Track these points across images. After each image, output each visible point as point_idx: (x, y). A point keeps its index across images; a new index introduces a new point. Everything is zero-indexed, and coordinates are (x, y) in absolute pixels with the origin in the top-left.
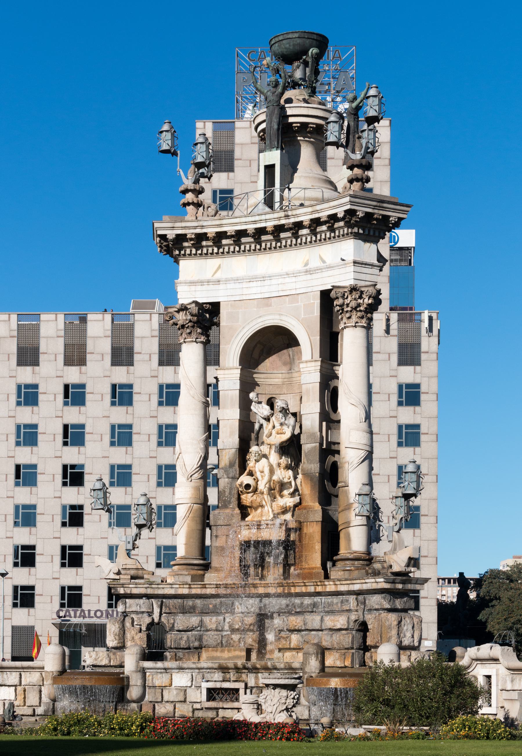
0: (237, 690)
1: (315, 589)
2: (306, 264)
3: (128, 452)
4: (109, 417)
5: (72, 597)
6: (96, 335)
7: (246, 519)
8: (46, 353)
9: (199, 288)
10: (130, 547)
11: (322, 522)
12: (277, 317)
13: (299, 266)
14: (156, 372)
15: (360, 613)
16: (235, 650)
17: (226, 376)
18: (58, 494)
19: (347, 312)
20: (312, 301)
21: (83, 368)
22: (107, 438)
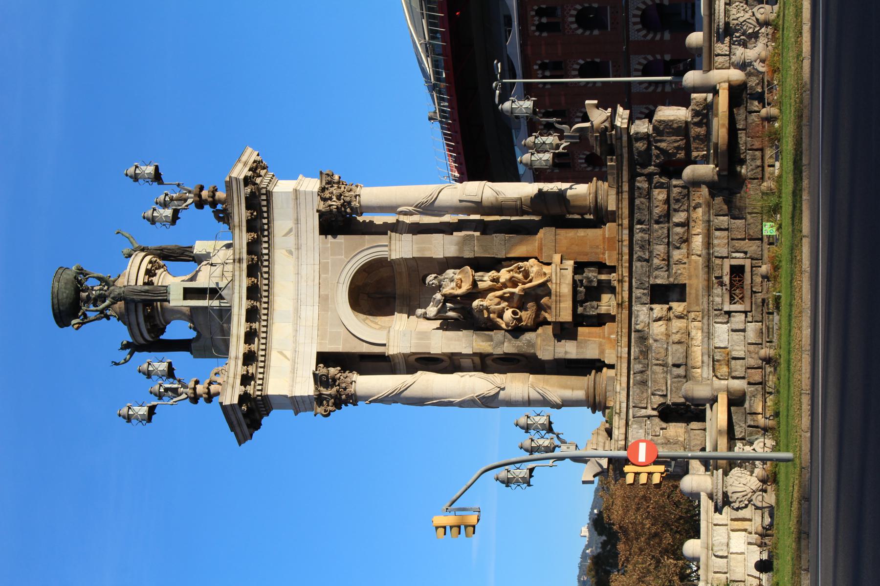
0: (732, 267)
2: (291, 253)
9: (300, 372)
11: (557, 227)
12: (341, 285)
13: (291, 260)
17: (396, 344)
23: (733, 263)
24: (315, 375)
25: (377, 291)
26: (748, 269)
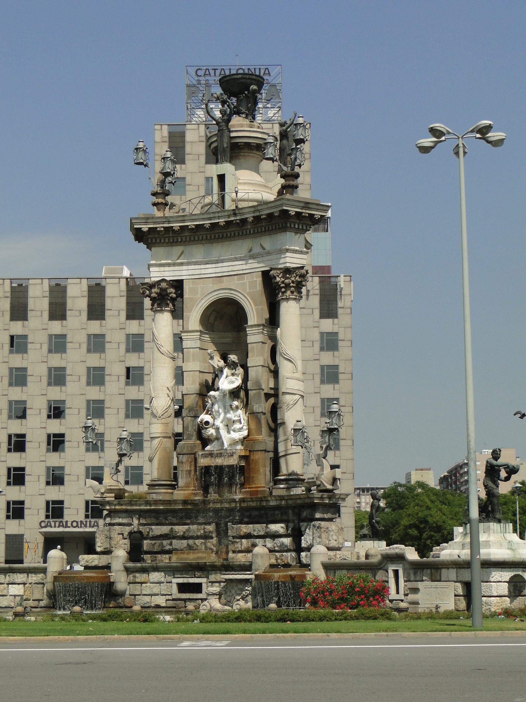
0: (200, 584)
1: (261, 503)
2: (250, 251)
3: (101, 391)
4: (85, 362)
5: (55, 510)
6: (75, 295)
7: (206, 449)
8: (34, 310)
9: (167, 269)
10: (114, 471)
12: (229, 291)
14: (124, 325)
15: (296, 522)
16: (198, 553)
17: (188, 337)
18: (43, 425)
19: (283, 287)
20: (255, 279)
21: (64, 322)
22: (84, 379)
23: (203, 584)
24: (163, 280)
25: (225, 320)
26: (199, 596)
